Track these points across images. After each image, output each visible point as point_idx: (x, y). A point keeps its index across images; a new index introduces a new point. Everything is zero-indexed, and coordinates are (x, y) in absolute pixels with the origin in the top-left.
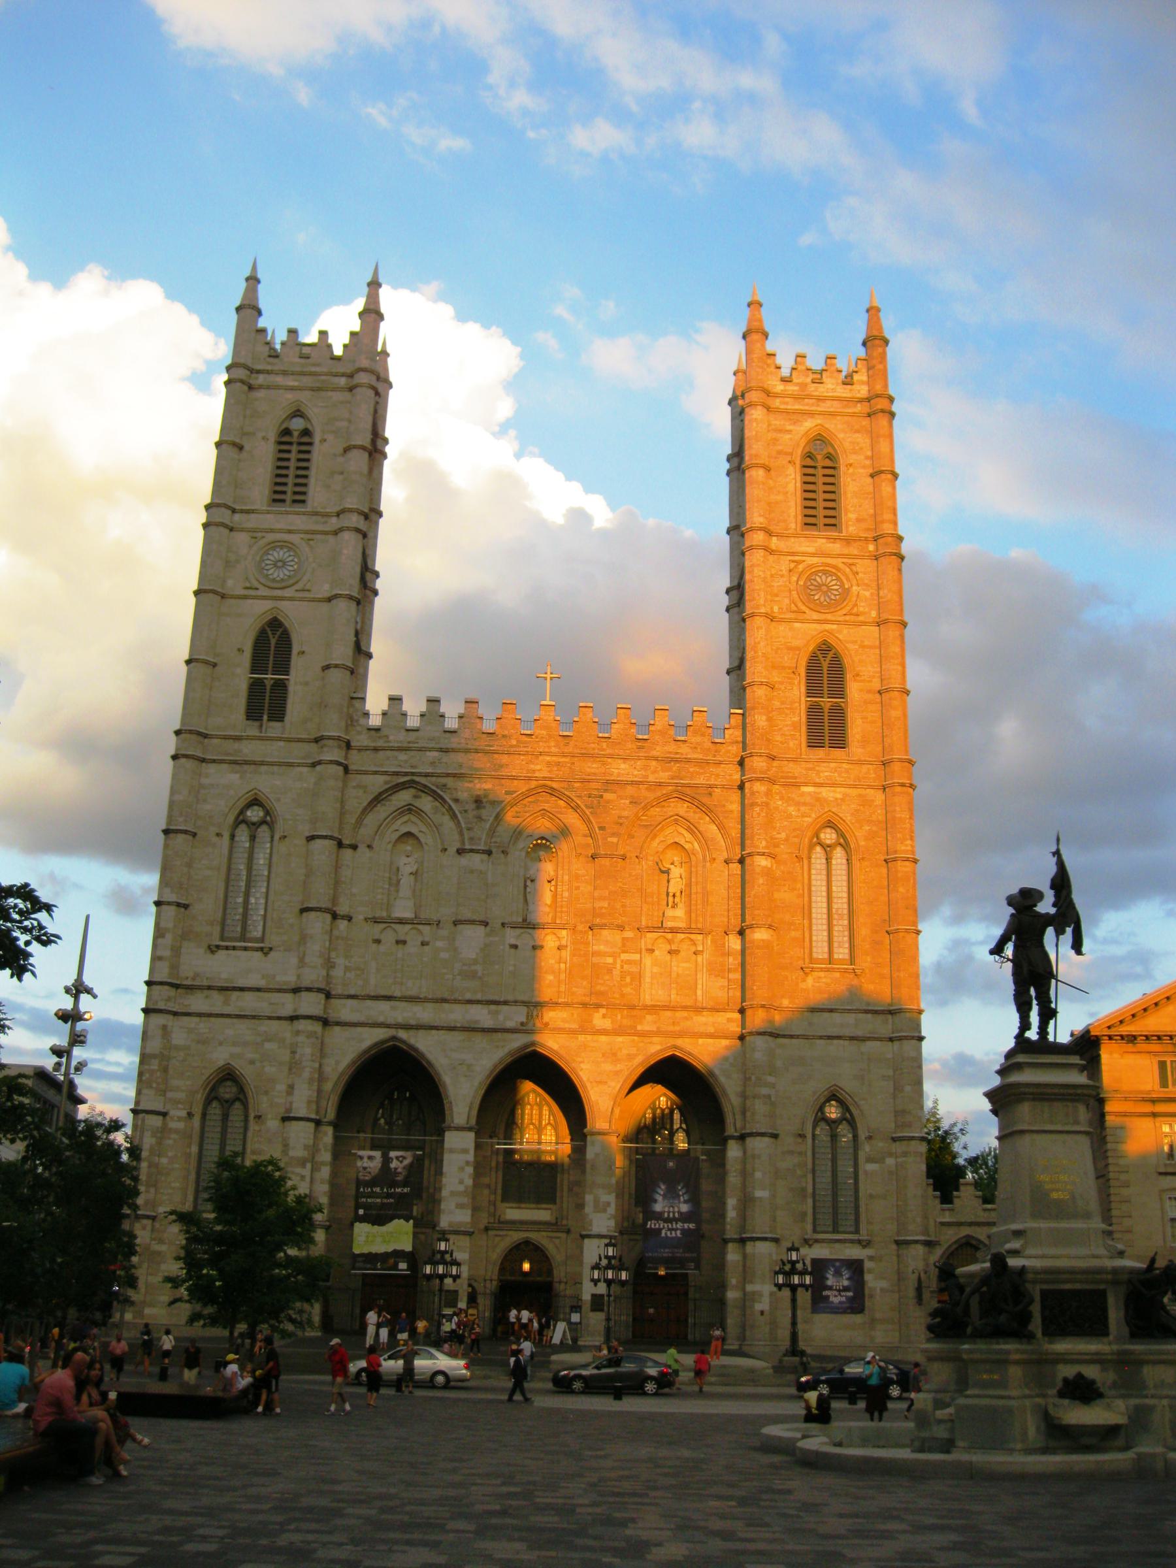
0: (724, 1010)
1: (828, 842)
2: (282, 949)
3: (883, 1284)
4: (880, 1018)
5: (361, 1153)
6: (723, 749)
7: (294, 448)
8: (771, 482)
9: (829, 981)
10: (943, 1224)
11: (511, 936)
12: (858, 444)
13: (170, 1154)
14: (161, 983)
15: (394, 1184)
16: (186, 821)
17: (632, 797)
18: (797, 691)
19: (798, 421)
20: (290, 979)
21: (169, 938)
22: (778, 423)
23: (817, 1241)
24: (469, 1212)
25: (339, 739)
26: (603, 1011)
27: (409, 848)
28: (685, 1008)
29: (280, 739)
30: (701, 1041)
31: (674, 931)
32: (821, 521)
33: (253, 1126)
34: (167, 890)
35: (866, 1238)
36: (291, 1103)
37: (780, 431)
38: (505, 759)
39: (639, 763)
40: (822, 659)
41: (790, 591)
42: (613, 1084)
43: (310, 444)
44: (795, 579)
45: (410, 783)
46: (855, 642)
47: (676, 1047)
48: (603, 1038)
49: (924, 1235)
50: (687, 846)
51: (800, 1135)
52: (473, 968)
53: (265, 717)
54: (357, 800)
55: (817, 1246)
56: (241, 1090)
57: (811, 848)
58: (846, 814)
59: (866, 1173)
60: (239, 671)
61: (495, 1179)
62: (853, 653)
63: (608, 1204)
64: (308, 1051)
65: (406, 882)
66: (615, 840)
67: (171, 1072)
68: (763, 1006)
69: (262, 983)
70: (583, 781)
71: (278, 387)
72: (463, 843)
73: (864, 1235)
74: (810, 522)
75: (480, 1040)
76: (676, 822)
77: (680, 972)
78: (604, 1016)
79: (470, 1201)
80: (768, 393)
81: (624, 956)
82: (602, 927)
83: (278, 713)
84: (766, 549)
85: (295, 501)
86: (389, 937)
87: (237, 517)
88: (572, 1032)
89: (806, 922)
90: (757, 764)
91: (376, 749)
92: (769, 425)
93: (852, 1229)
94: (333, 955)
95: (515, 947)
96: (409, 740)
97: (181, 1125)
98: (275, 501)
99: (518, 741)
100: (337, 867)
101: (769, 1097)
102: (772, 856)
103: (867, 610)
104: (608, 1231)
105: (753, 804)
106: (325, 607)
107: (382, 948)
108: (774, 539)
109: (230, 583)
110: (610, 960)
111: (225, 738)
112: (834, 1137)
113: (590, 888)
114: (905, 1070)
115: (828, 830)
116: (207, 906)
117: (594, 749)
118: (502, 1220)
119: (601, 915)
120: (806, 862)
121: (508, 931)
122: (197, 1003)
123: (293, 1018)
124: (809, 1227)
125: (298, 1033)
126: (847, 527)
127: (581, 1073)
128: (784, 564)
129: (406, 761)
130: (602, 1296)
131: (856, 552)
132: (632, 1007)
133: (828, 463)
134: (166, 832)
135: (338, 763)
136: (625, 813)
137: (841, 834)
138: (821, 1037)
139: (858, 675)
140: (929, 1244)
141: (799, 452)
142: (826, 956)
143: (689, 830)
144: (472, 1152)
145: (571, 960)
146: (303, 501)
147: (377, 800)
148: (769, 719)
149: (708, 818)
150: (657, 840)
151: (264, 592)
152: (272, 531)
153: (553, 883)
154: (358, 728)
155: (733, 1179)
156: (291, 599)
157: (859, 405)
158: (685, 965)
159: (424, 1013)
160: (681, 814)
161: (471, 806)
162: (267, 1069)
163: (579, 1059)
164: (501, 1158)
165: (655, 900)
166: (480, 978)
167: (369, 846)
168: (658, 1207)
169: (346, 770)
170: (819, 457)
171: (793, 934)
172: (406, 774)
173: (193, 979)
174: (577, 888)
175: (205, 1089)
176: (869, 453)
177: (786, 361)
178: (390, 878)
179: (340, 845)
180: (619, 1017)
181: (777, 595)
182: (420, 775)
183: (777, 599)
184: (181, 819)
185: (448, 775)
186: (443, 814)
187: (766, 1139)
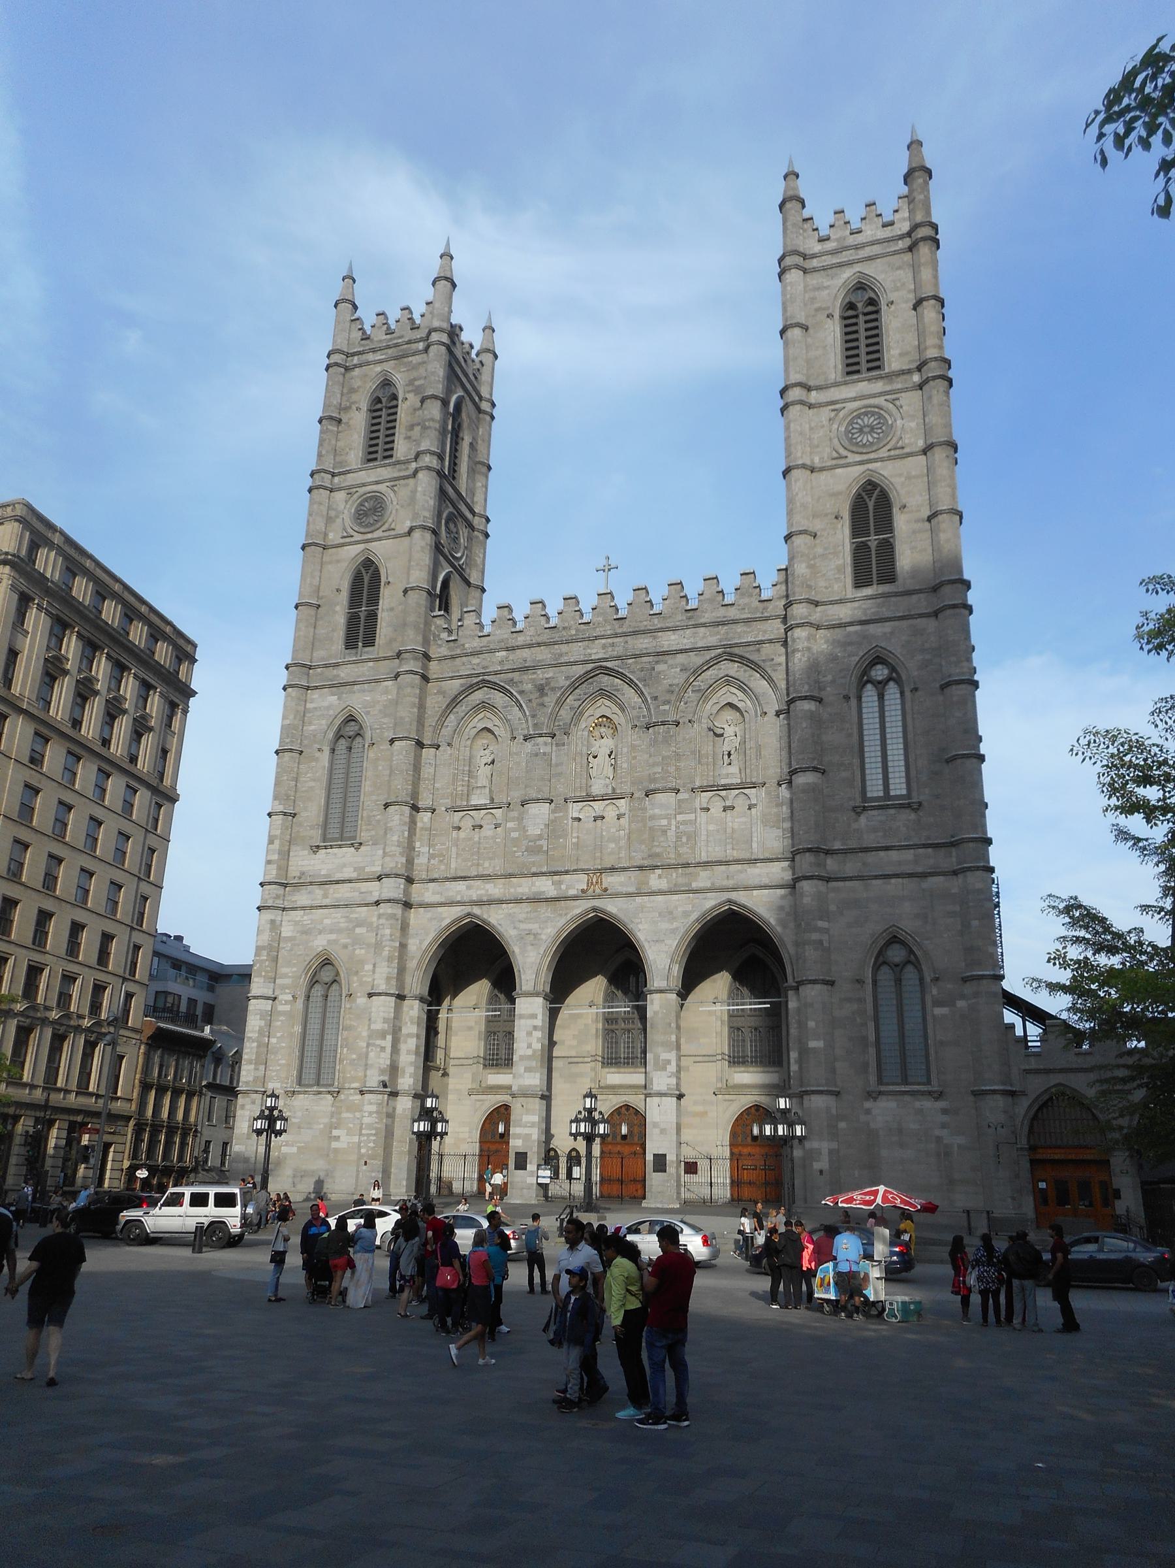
0: (778, 860)
1: (880, 678)
3: (960, 1140)
6: (771, 606)
7: (384, 413)
8: (809, 340)
9: (883, 818)
10: (1028, 1071)
11: (574, 810)
12: (900, 280)
13: (279, 1035)
14: (270, 883)
16: (292, 742)
17: (683, 665)
18: (841, 537)
19: (836, 274)
20: (377, 869)
21: (277, 842)
22: (815, 282)
23: (880, 1093)
24: (538, 1075)
25: (413, 651)
26: (659, 872)
27: (485, 741)
28: (738, 861)
29: (370, 660)
30: (755, 893)
31: (727, 788)
32: (864, 366)
33: (346, 1004)
34: (277, 802)
35: (936, 1089)
36: (374, 980)
37: (818, 289)
38: (564, 648)
39: (688, 631)
40: (866, 497)
41: (831, 439)
42: (668, 942)
43: (396, 406)
44: (835, 426)
45: (484, 683)
46: (900, 475)
47: (730, 901)
48: (660, 898)
49: (1004, 1084)
50: (740, 705)
51: (858, 981)
52: (541, 842)
53: (360, 644)
54: (435, 703)
55: (884, 1098)
56: (337, 974)
57: (862, 685)
58: (896, 648)
59: (934, 1016)
60: (338, 608)
61: (594, 1046)
62: (898, 488)
63: (669, 1062)
64: (388, 932)
65: (483, 773)
66: (667, 707)
67: (280, 961)
68: (809, 850)
69: (354, 875)
70: (636, 656)
71: (368, 363)
72: (529, 731)
73: (935, 1087)
74: (852, 368)
75: (545, 910)
76: (728, 683)
77: (736, 827)
78: (660, 877)
79: (539, 1064)
80: (805, 257)
81: (680, 818)
82: (655, 791)
83: (370, 641)
84: (802, 402)
85: (385, 457)
86: (467, 824)
87: (336, 479)
88: (629, 895)
89: (856, 761)
90: (799, 611)
91: (453, 657)
92: (805, 287)
93: (924, 1080)
94: (418, 844)
97: (287, 1008)
98: (369, 460)
99: (577, 630)
100: (417, 767)
101: (821, 942)
102: (820, 701)
103: (913, 440)
105: (794, 651)
106: (407, 540)
107: (462, 834)
108: (814, 393)
109: (331, 536)
110: (664, 822)
111: (326, 666)
112: (898, 981)
113: (646, 756)
114: (971, 904)
115: (879, 667)
116: (311, 812)
118: (602, 1085)
119: (654, 780)
120: (854, 702)
121: (571, 805)
122: (302, 898)
123: (377, 903)
124: (873, 1078)
125: (380, 916)
126: (890, 365)
127: (638, 934)
128: (826, 413)
129: (478, 664)
130: (665, 1155)
131: (899, 386)
132: (686, 865)
133: (870, 308)
134: (277, 752)
135: (416, 673)
136: (676, 681)
137: (893, 669)
138: (876, 877)
139: (905, 507)
140: (1012, 1094)
141: (838, 304)
142: (881, 794)
143: (740, 688)
144: (540, 1017)
145: (629, 825)
146: (391, 456)
147: (454, 702)
148: (811, 567)
150: (710, 703)
151: (358, 537)
152: (364, 485)
154: (439, 642)
155: (793, 1031)
156: (379, 539)
157: (900, 242)
158: (739, 820)
159: (494, 889)
160: (732, 673)
162: (357, 952)
163: (637, 921)
164: (600, 1026)
165: (711, 760)
166: (544, 852)
167: (449, 745)
169: (425, 678)
170: (860, 305)
171: (844, 774)
172: (478, 675)
173: (300, 878)
174: (635, 758)
176: (912, 287)
177: (823, 220)
178: (469, 771)
179: (420, 744)
180: (674, 875)
181: (818, 446)
182: (489, 674)
183: (818, 449)
184: (287, 740)
185: (514, 670)
186: (513, 706)
187: (818, 987)
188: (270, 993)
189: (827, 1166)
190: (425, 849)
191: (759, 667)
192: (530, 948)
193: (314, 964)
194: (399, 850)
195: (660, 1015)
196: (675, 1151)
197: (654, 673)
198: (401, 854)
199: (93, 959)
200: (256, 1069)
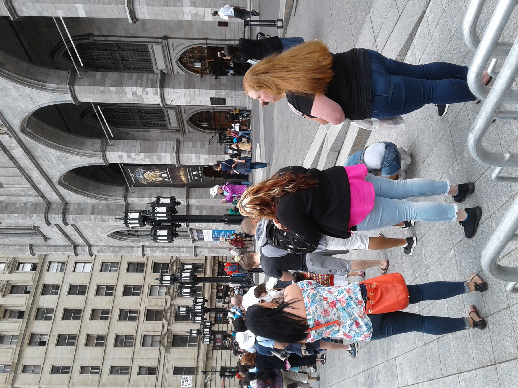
24: (163, 155)
63: (134, 93)
79: (155, 154)
104: (157, 95)
144: (120, 154)
163: (19, 110)
175: (125, 239)
188: (141, 248)
189: (209, 9)
190: (23, 198)
192: (70, 159)
193: (118, 237)
194: (28, 218)
195: (96, 98)
196: (208, 91)
198: (31, 217)
199: (140, 275)
200: (183, 252)
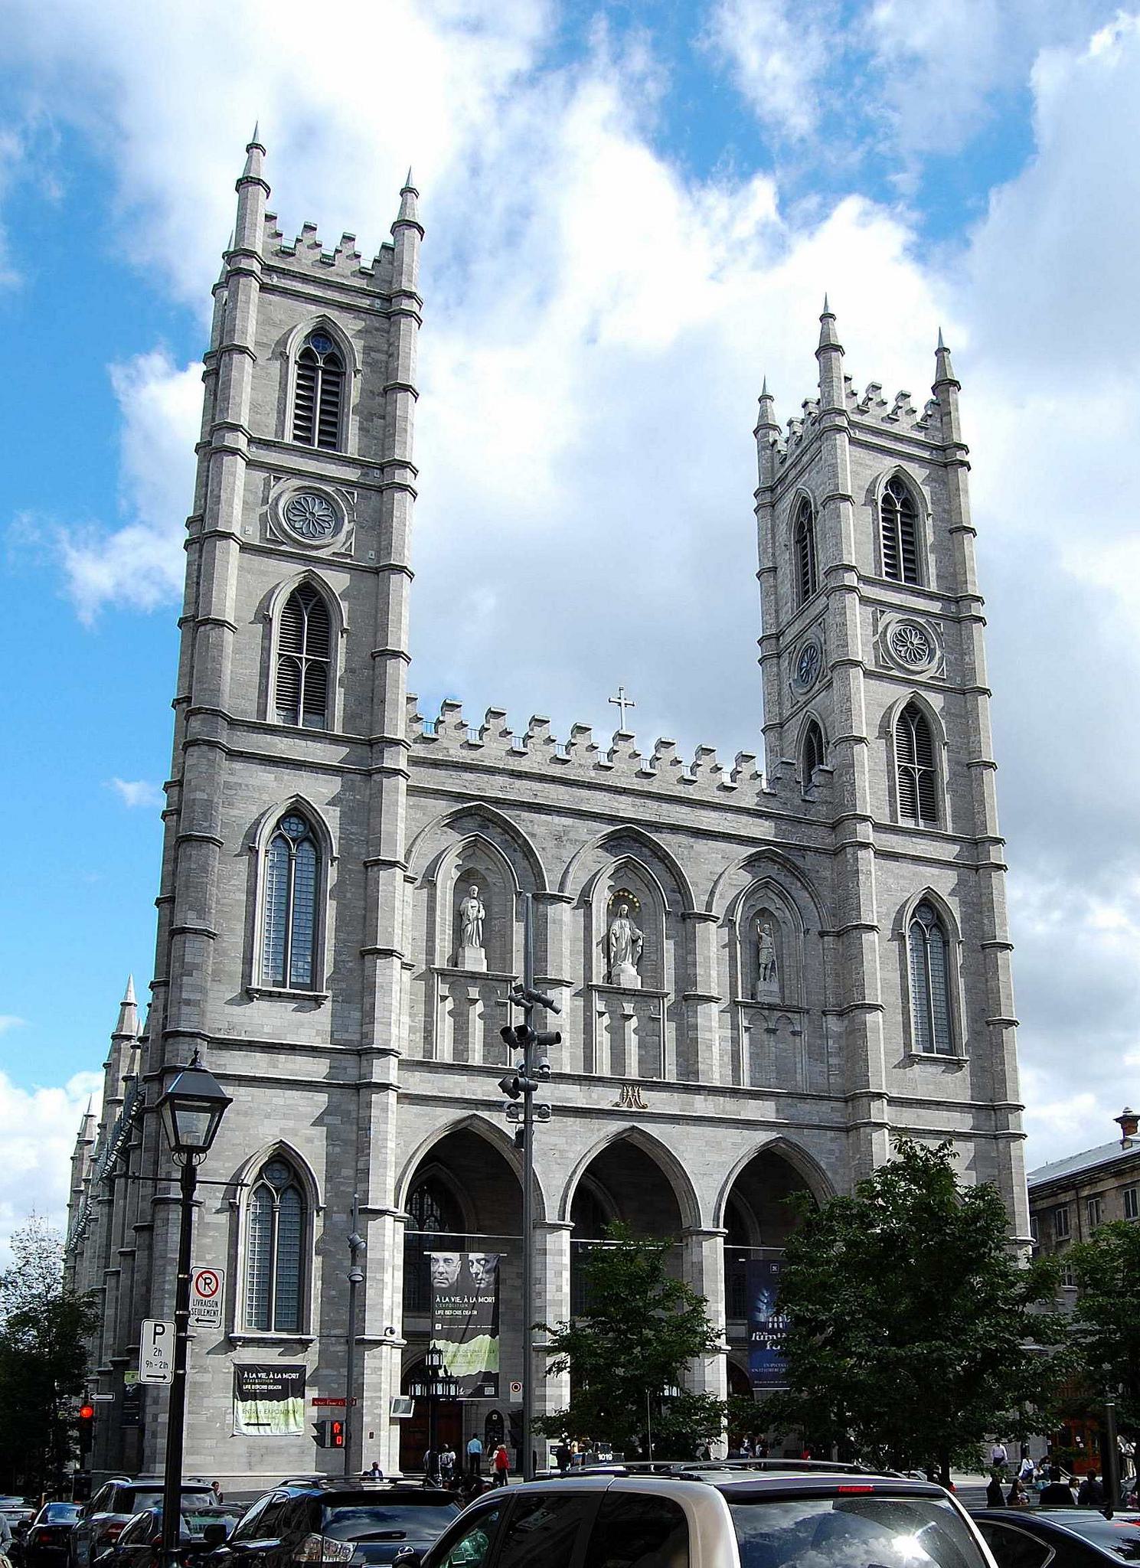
0: (829, 1099)
2: (340, 999)
4: (983, 1114)
5: (434, 1255)
15: (478, 1293)
31: (771, 1007)
38: (585, 793)
95: (601, 1014)
96: (473, 756)
110: (707, 1035)
117: (680, 792)
143: (779, 895)
149: (799, 884)
153: (640, 942)
161: (550, 844)
168: (762, 1317)
191: (804, 876)
197: (692, 853)
